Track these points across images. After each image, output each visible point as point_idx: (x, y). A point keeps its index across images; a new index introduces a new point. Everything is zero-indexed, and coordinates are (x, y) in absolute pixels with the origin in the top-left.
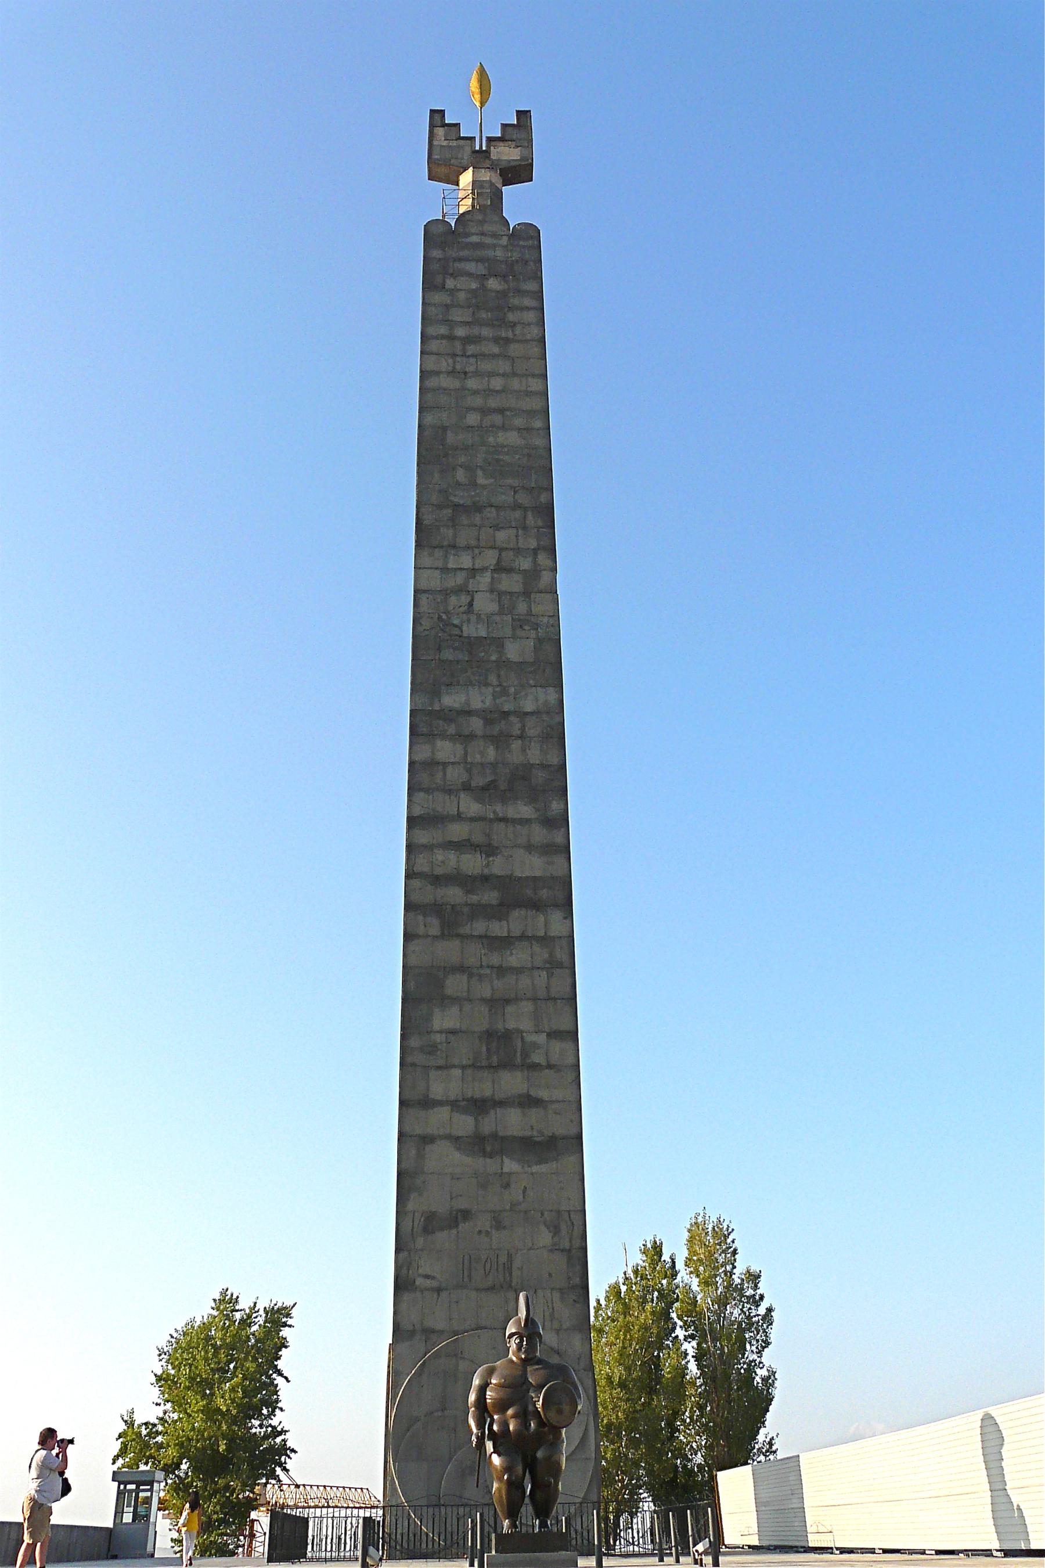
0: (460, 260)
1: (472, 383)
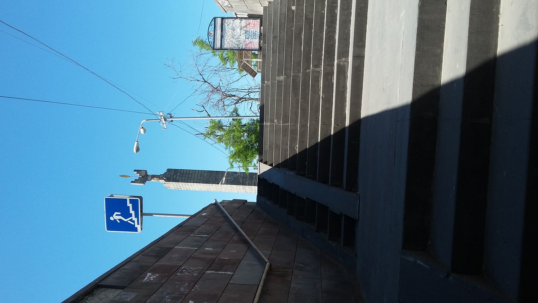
1: (196, 177)
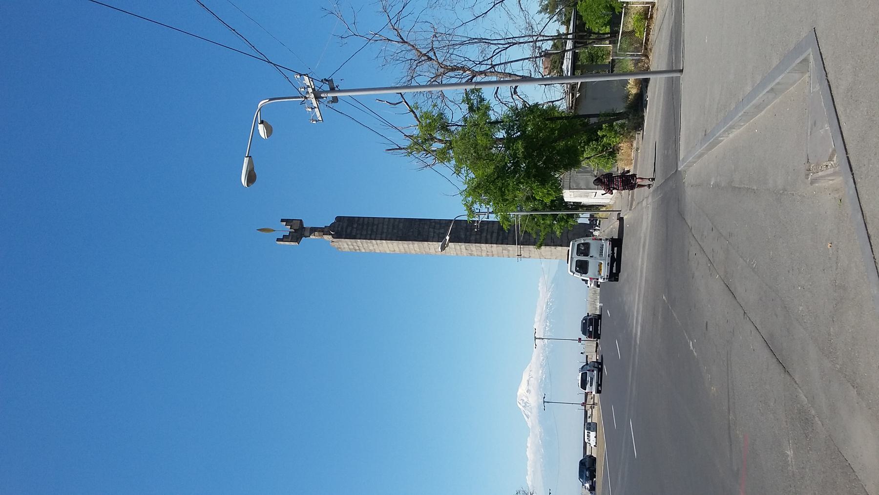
1: (385, 231)
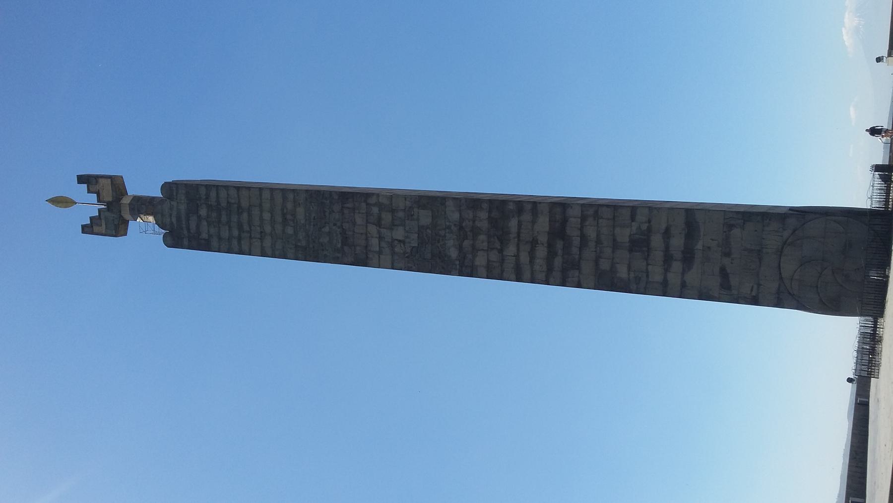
0: (188, 229)
1: (268, 229)
